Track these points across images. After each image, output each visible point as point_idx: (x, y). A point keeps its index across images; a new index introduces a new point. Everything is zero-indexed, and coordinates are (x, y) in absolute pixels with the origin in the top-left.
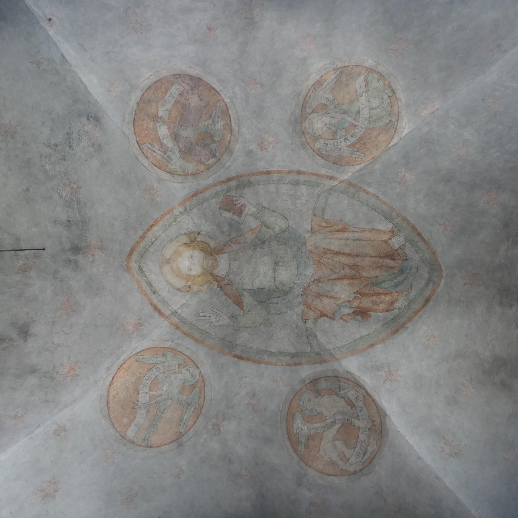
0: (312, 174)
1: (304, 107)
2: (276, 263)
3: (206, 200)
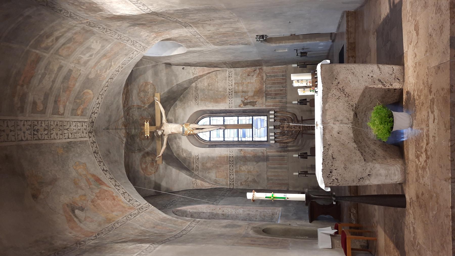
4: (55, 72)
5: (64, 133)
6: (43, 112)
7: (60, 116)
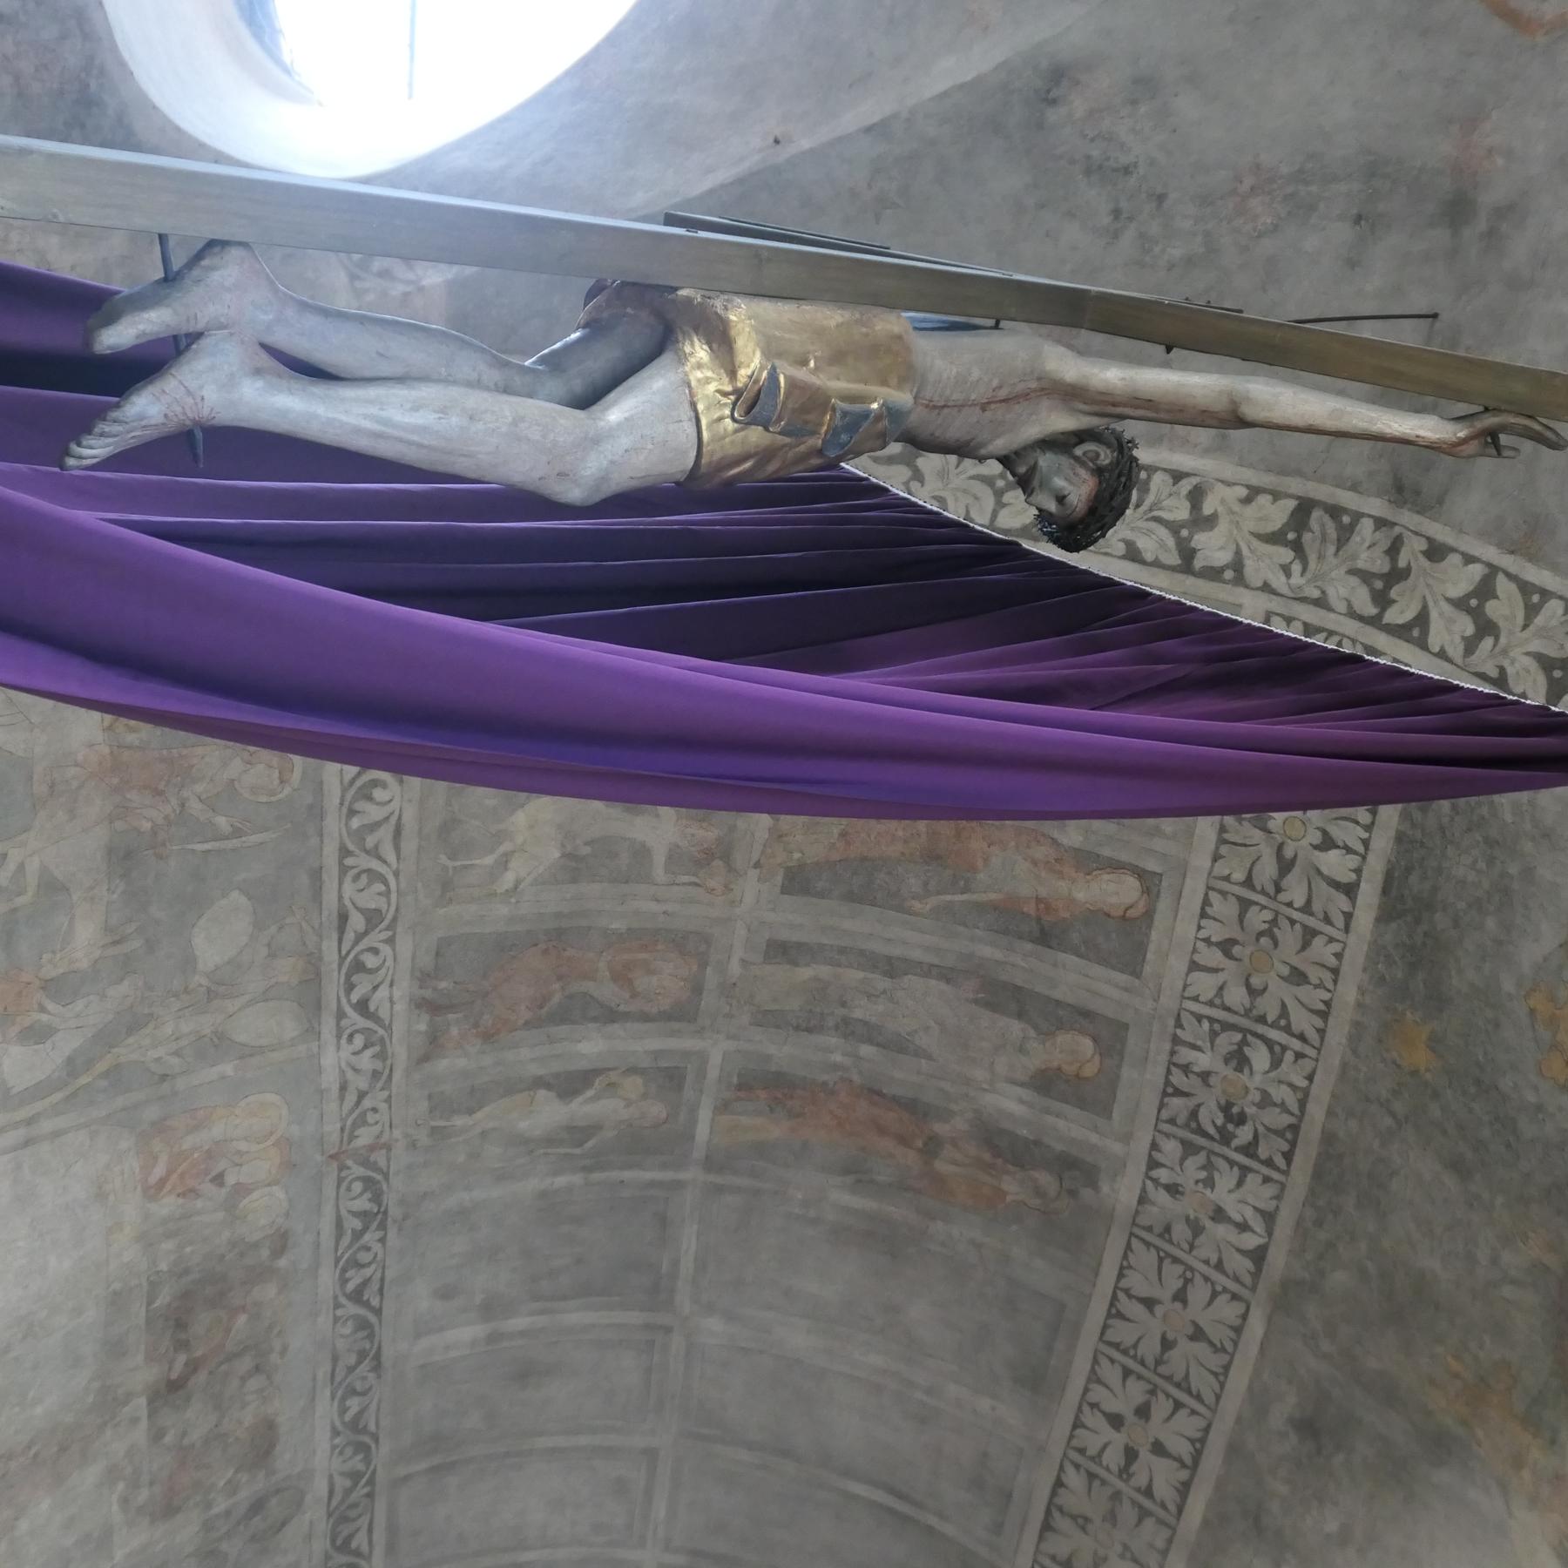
4: (824, 971)
5: (1307, 909)
6: (1112, 1037)
7: (1163, 906)
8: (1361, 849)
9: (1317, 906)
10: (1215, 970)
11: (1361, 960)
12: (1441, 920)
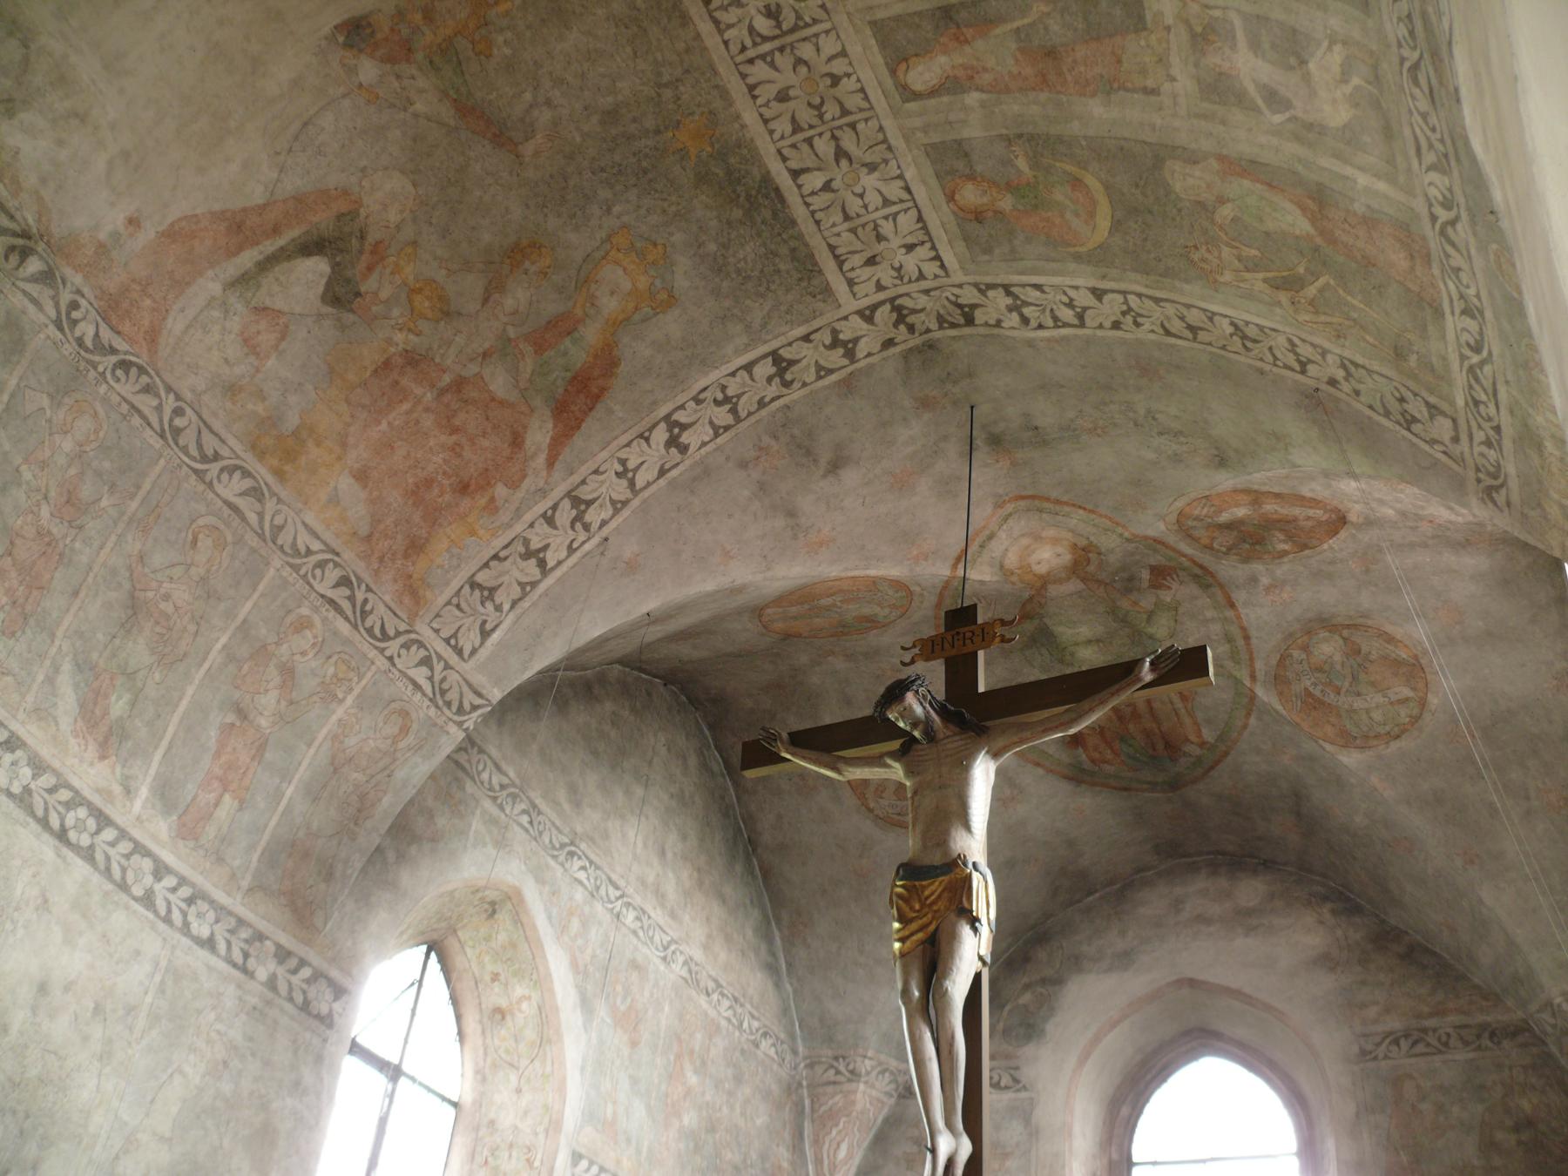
0: (1251, 654)
1: (1348, 627)
2: (1098, 641)
3: (1155, 550)
5: (809, 141)
7: (889, 82)
8: (809, 200)
9: (805, 147)
10: (830, 59)
11: (759, 143)
12: (737, 213)
